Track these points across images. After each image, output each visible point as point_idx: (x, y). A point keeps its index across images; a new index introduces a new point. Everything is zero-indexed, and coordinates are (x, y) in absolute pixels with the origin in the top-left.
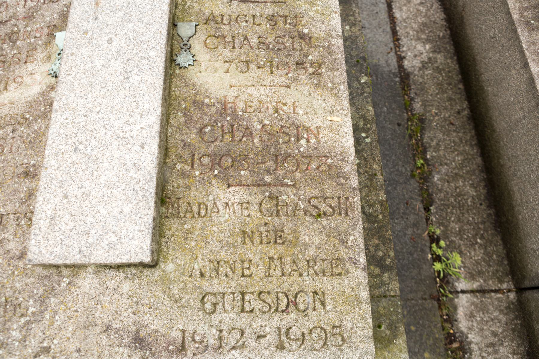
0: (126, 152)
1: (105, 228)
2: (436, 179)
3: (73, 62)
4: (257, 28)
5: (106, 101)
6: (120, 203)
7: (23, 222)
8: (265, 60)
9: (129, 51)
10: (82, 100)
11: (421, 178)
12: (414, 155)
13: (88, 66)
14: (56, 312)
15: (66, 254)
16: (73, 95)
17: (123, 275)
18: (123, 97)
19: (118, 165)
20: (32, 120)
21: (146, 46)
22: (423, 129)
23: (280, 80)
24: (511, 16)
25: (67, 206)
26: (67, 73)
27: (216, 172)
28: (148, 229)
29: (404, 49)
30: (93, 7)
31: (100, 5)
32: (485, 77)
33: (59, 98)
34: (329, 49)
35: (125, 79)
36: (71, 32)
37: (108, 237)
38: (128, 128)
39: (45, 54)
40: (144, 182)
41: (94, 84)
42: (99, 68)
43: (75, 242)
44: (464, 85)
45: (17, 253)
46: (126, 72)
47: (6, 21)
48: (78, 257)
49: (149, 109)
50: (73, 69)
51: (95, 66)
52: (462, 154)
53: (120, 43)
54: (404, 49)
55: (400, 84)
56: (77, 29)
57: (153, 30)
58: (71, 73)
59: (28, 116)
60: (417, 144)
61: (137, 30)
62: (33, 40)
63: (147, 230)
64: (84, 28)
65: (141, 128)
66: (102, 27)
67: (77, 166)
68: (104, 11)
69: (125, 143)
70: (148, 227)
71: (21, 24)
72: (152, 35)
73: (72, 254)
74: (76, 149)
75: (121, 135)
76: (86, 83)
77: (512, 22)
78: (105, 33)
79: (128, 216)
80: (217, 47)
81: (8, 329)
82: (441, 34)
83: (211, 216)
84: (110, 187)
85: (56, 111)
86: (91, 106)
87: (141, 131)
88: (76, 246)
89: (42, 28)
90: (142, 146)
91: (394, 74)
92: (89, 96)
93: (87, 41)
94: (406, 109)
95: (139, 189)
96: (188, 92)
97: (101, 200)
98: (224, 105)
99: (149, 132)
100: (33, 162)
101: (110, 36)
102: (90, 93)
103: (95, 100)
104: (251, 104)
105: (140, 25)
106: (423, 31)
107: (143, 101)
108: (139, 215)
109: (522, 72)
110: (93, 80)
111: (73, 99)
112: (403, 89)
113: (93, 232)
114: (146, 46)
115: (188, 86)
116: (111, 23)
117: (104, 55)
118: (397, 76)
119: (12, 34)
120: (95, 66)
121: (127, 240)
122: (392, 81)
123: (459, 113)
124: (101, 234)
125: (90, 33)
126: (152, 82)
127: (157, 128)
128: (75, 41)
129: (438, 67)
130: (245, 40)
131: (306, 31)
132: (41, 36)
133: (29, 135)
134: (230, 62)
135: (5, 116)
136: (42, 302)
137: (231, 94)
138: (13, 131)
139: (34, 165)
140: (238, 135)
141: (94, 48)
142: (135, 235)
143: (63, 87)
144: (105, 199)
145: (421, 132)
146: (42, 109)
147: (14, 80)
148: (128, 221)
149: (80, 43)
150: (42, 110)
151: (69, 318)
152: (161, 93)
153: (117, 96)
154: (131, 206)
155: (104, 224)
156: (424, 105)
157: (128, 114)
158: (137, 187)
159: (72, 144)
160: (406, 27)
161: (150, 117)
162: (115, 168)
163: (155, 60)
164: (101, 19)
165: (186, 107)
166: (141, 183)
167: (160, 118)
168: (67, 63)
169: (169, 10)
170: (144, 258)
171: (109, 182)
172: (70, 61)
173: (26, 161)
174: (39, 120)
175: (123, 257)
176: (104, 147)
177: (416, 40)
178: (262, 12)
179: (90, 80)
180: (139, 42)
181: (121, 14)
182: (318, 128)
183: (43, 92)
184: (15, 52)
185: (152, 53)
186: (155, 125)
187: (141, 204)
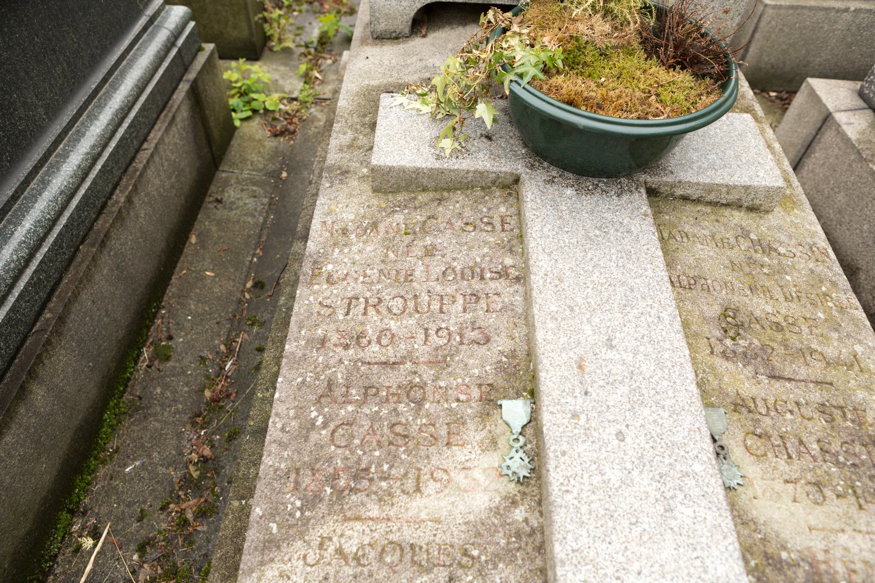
3: (569, 469)
4: (810, 424)
5: (646, 551)
8: (842, 483)
9: (657, 458)
10: (604, 546)
13: (597, 479)
16: (585, 534)
18: (675, 546)
20: (486, 561)
21: (683, 453)
26: (564, 488)
30: (576, 373)
31: (587, 370)
33: (560, 536)
35: (666, 511)
36: (552, 413)
39: (484, 433)
41: (616, 515)
42: (617, 485)
46: (665, 498)
47: (394, 363)
49: (727, 577)
50: (571, 480)
53: (638, 441)
56: (559, 407)
57: (686, 425)
58: (570, 488)
59: (475, 553)
62: (454, 405)
64: (572, 408)
66: (599, 409)
68: (595, 382)
71: (428, 374)
76: (602, 512)
78: (609, 422)
80: (765, 455)
85: (563, 563)
86: (623, 559)
89: (468, 386)
92: (614, 537)
93: (582, 431)
96: (750, 536)
98: (813, 564)
101: (618, 427)
102: (614, 532)
103: (626, 548)
104: (852, 566)
105: (660, 412)
107: (711, 559)
110: (612, 508)
111: (586, 541)
114: (683, 453)
115: (747, 524)
117: (617, 461)
119: (412, 388)
125: (583, 417)
126: (715, 523)
128: (561, 429)
130: (800, 444)
132: (468, 401)
134: (792, 482)
135: (427, 544)
137: (817, 544)
141: (598, 446)
143: (562, 515)
146: (503, 542)
147: (432, 474)
149: (571, 434)
150: (502, 544)
153: (662, 544)
164: (594, 395)
165: (756, 564)
172: (563, 467)
174: (501, 565)
178: (807, 398)
179: (607, 506)
180: (670, 444)
181: (625, 389)
183: (498, 508)
184: (424, 421)
185: (697, 467)
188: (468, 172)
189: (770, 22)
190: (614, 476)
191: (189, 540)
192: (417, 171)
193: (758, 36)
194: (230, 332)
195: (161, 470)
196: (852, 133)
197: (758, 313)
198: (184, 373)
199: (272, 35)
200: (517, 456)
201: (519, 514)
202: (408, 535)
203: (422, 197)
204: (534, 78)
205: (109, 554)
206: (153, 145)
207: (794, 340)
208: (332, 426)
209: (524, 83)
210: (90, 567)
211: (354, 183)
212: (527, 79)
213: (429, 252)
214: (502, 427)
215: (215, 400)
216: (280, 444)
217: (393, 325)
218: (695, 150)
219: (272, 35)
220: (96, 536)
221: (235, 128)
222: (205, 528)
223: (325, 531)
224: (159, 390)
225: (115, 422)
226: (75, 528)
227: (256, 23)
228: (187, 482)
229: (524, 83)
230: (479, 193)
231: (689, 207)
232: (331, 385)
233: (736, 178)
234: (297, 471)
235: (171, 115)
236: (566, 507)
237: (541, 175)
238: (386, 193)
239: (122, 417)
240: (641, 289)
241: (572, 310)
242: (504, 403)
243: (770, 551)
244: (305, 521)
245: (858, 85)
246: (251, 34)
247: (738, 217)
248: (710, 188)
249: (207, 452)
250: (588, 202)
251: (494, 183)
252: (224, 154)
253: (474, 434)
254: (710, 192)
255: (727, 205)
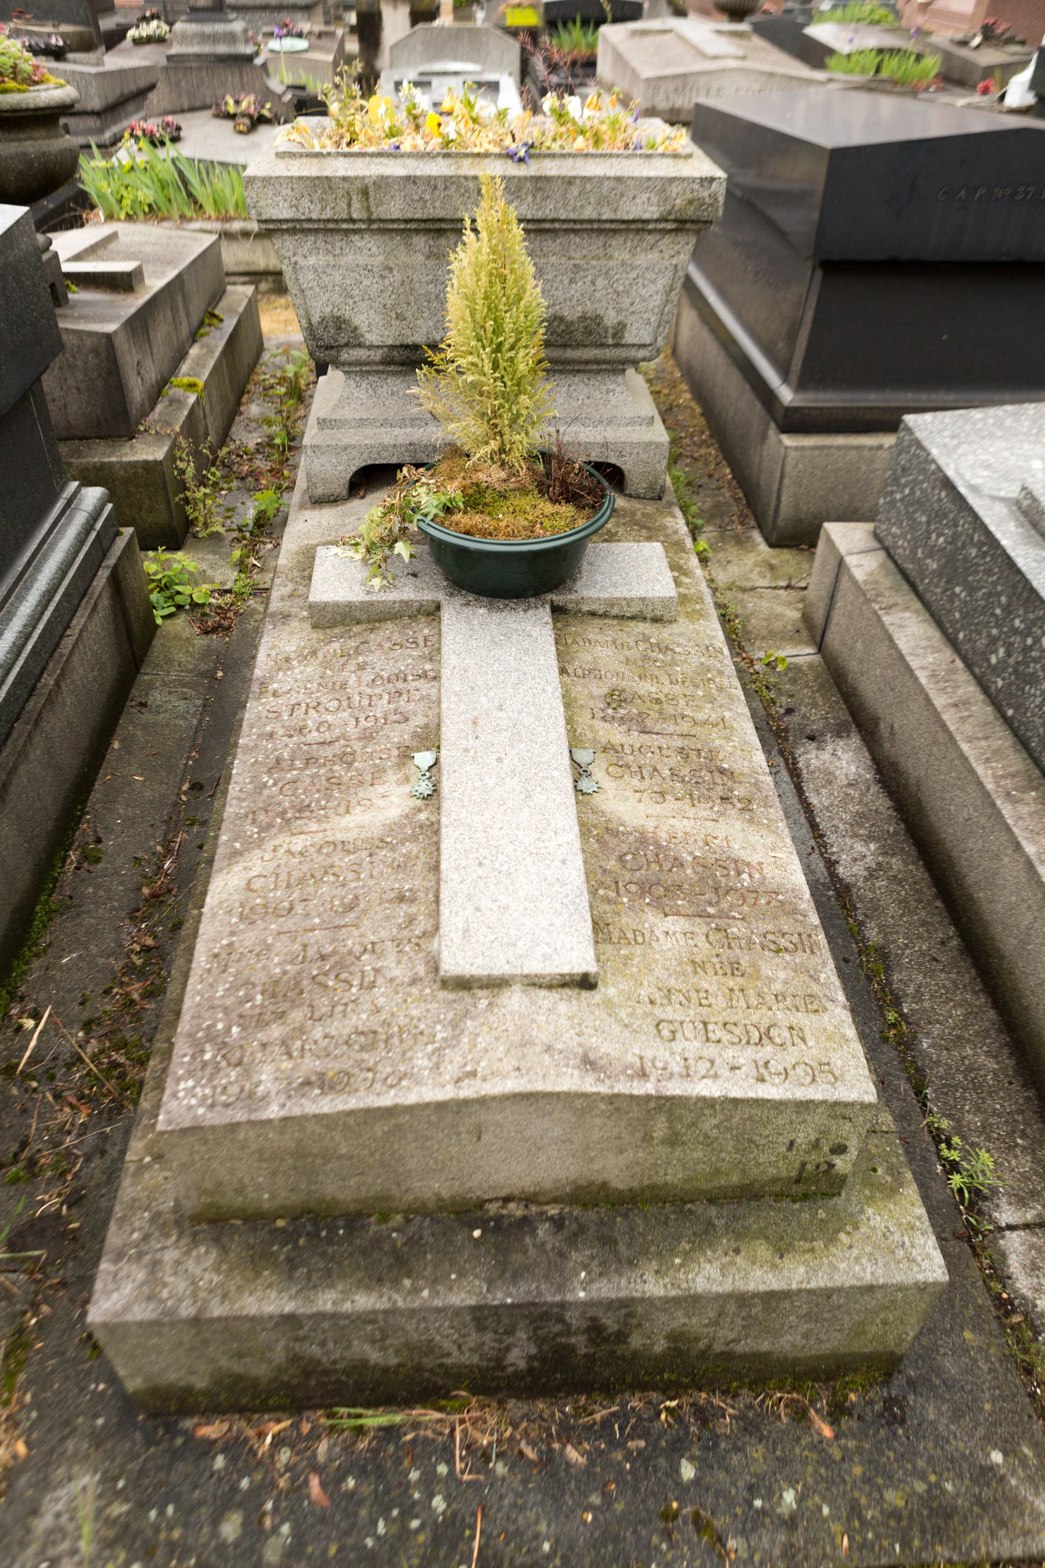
2: (925, 1045)
7: (407, 949)
11: (899, 1044)
12: (881, 1008)
14: (477, 1035)
17: (558, 996)
22: (888, 969)
23: (706, 813)
24: (983, 787)
27: (647, 900)
29: (834, 849)
32: (970, 879)
34: (757, 784)
38: (542, 845)
44: (944, 901)
45: (406, 980)
48: (507, 967)
52: (961, 1006)
54: (834, 849)
55: (837, 899)
57: (552, 751)
59: (389, 840)
60: (883, 990)
71: (357, 746)
74: (480, 864)
77: (987, 795)
81: (411, 1059)
82: (891, 829)
90: (564, 862)
91: (823, 884)
94: (852, 935)
100: (407, 887)
106: (861, 825)
109: (1016, 856)
112: (844, 907)
113: (520, 944)
118: (829, 889)
122: (823, 895)
123: (943, 943)
125: (472, 752)
129: (895, 877)
131: (726, 766)
133: (394, 859)
136: (455, 1027)
137: (650, 825)
138: (370, 855)
139: (410, 890)
140: (667, 866)
145: (886, 972)
151: (497, 1039)
156: (882, 928)
158: (566, 901)
160: (831, 818)
173: (397, 886)
177: (852, 837)
182: (760, 864)
185: (555, 773)
188: (394, 602)
189: (796, 466)
190: (491, 781)
191: (137, 1017)
192: (350, 605)
193: (786, 481)
194: (166, 834)
195: (101, 961)
196: (859, 575)
197: (642, 692)
198: (117, 873)
199: (196, 518)
200: (423, 784)
201: (422, 816)
202: (339, 836)
203: (356, 629)
204: (436, 516)
205: (52, 1033)
206: (77, 631)
207: (670, 710)
208: (280, 784)
209: (428, 520)
210: (33, 1043)
211: (295, 624)
212: (430, 517)
213: (361, 667)
214: (413, 769)
215: (154, 896)
216: (239, 799)
217: (329, 718)
218: (602, 573)
219: (196, 518)
220: (37, 1016)
221: (157, 627)
222: (153, 1006)
223: (276, 842)
224: (91, 890)
225: (45, 919)
226: (13, 1012)
227: (177, 504)
228: (130, 969)
229: (428, 520)
230: (406, 619)
231: (596, 621)
232: (278, 761)
234: (254, 813)
235: (92, 602)
237: (458, 600)
238: (324, 628)
239: (53, 915)
241: (472, 688)
242: (417, 755)
243: (610, 826)
244: (262, 840)
245: (869, 526)
246: (171, 518)
247: (642, 627)
248: (612, 602)
249: (149, 942)
250: (497, 617)
251: (419, 611)
252: (145, 654)
253: (392, 776)
254: (612, 605)
255: (633, 618)
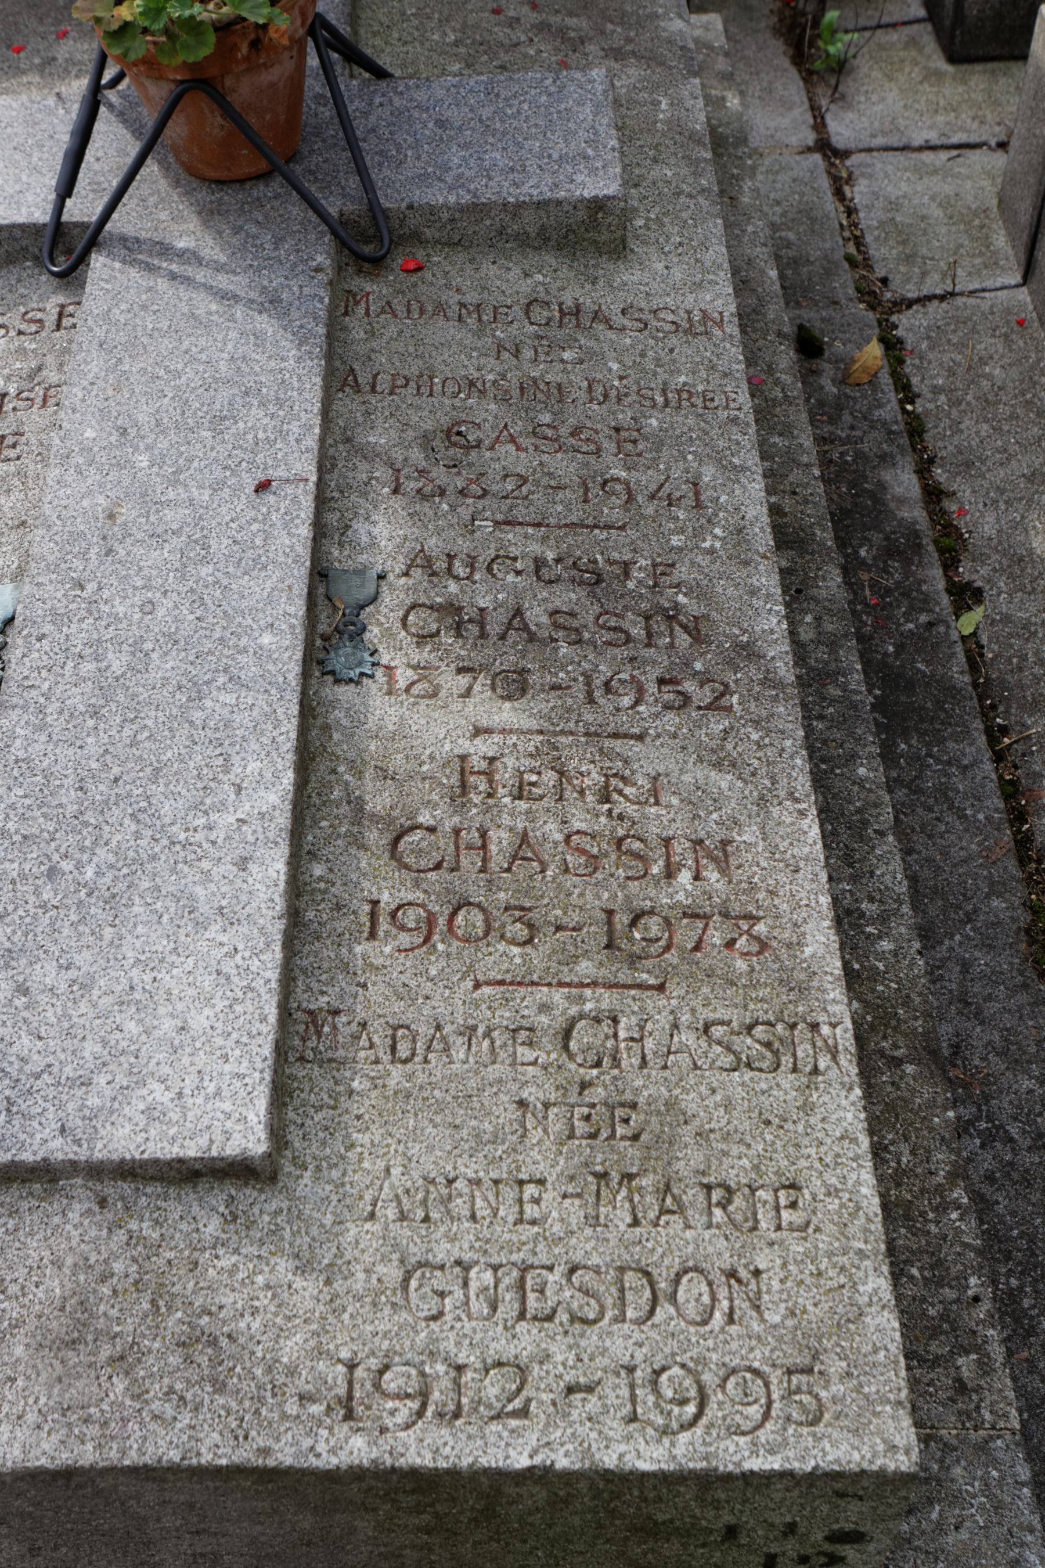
0: (196, 879)
1: (135, 1070)
6: (180, 1006)
9: (202, 632)
10: (71, 752)
13: (88, 667)
15: (22, 1137)
19: (172, 910)
25: (26, 1014)
28: (261, 1072)
37: (144, 1092)
40: (247, 954)
42: (119, 673)
43: (48, 1105)
48: (58, 1142)
51: (108, 667)
61: (225, 582)
63: (257, 1075)
65: (238, 820)
67: (54, 912)
69: (193, 856)
70: (259, 1065)
72: (265, 594)
73: (38, 1136)
75: (182, 836)
79: (203, 1039)
83: (426, 1061)
84: (152, 965)
86: (94, 765)
87: (239, 828)
88: (51, 1116)
95: (234, 971)
97: (126, 998)
99: (260, 830)
107: (243, 755)
108: (235, 1036)
110: (102, 702)
111: (43, 747)
113: (102, 1080)
116: (149, 563)
117: (131, 641)
120: (108, 667)
121: (200, 1100)
124: (125, 1084)
125: (91, 587)
127: (283, 819)
142: (224, 1087)
144: (137, 995)
148: (201, 1053)
152: (293, 735)
154: (212, 1014)
155: (132, 1060)
157: (200, 785)
158: (228, 967)
159: (42, 859)
161: (262, 793)
162: (165, 919)
163: (275, 656)
166: (238, 957)
167: (290, 796)
168: (26, 659)
169: (311, 535)
170: (250, 1145)
171: (148, 955)
175: (187, 1142)
176: (134, 868)
186: (277, 813)
187: (239, 1009)
233: (525, 189)
236: (22, 707)
240: (264, 390)
241: (124, 432)
